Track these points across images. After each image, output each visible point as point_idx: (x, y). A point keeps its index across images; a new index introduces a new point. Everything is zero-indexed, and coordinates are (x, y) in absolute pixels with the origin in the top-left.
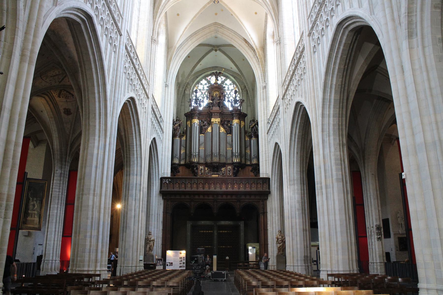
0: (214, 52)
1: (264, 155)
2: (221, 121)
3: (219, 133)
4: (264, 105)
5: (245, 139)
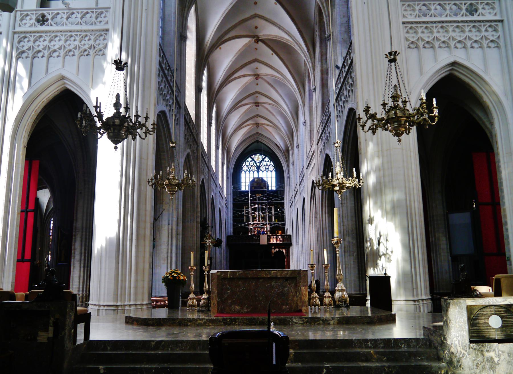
1: (288, 220)
4: (288, 189)
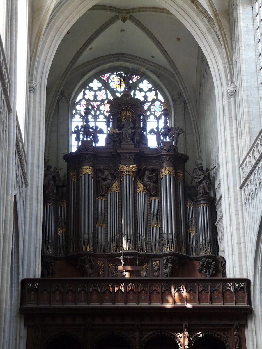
1: (235, 232)
4: (231, 130)
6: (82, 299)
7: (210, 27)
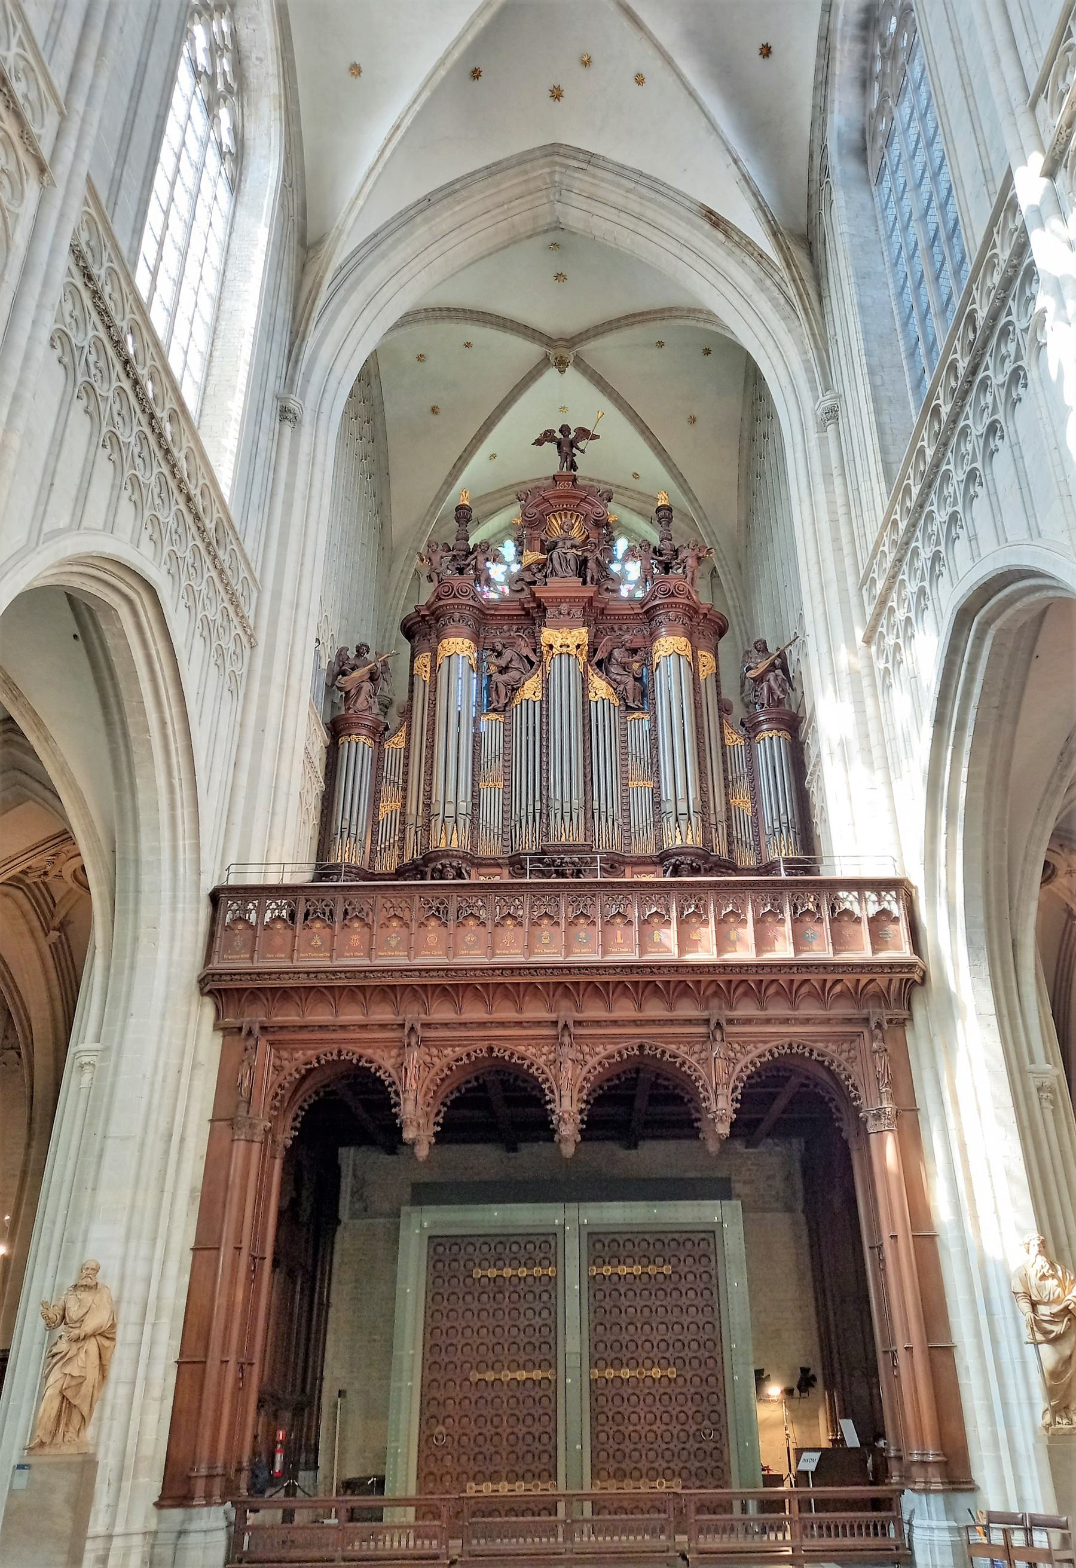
0: (552, 373)
2: (593, 650)
3: (586, 703)
4: (831, 502)
5: (723, 739)
6: (393, 943)
7: (762, 275)
